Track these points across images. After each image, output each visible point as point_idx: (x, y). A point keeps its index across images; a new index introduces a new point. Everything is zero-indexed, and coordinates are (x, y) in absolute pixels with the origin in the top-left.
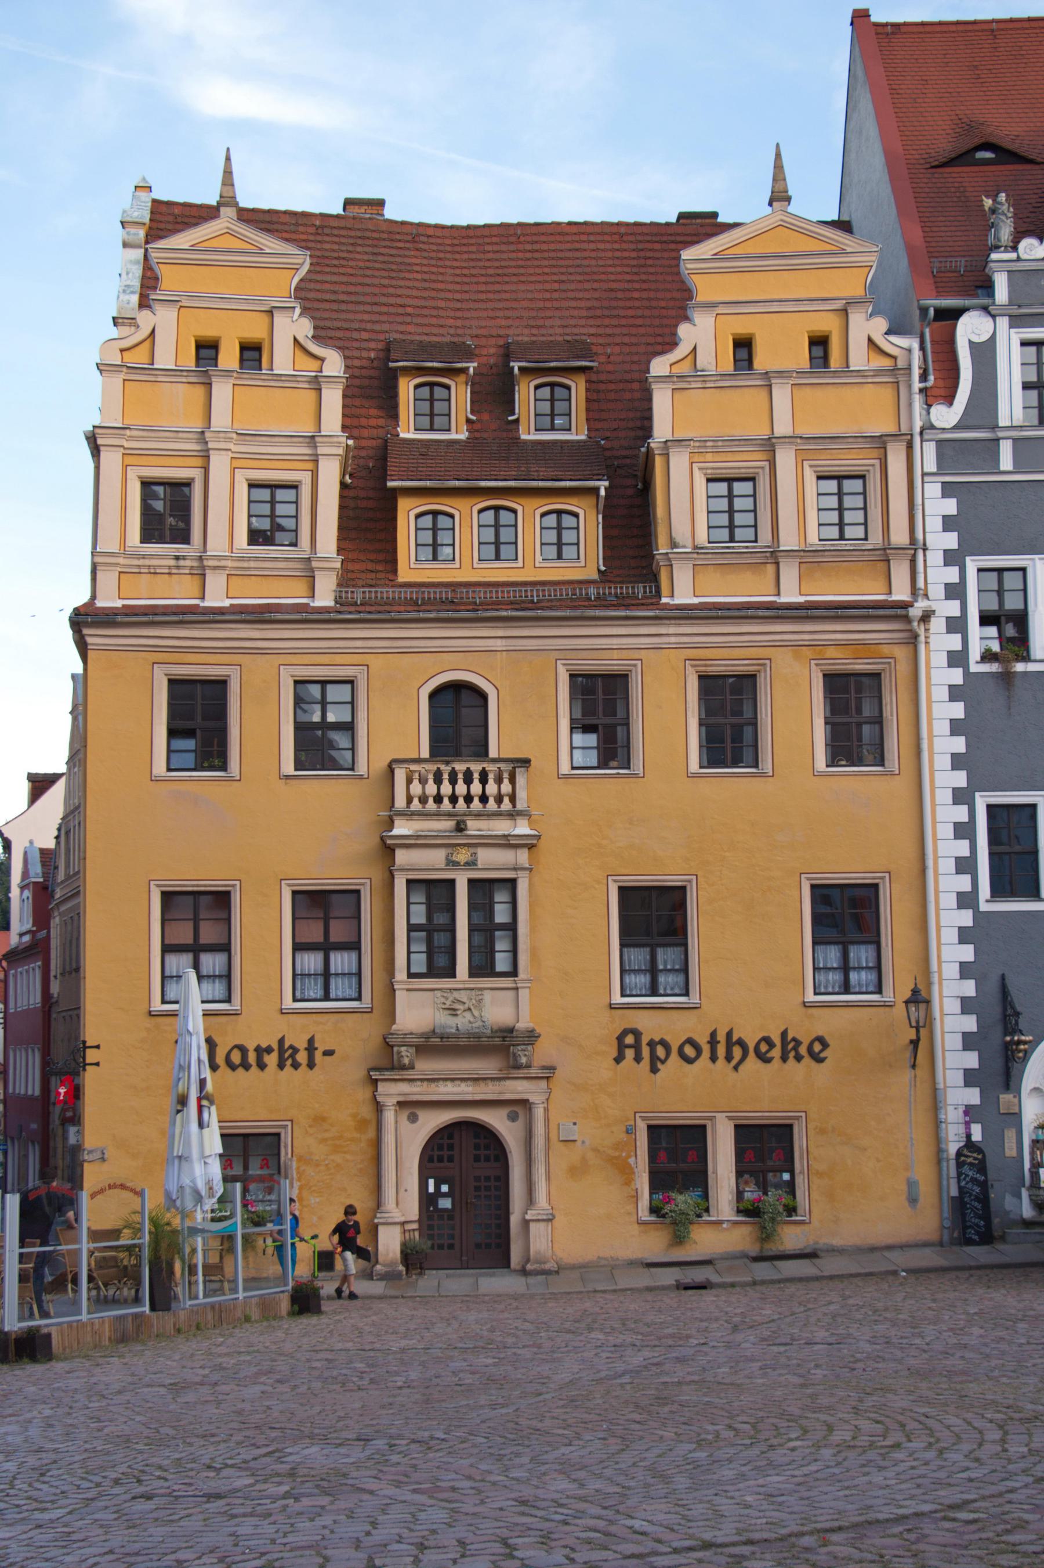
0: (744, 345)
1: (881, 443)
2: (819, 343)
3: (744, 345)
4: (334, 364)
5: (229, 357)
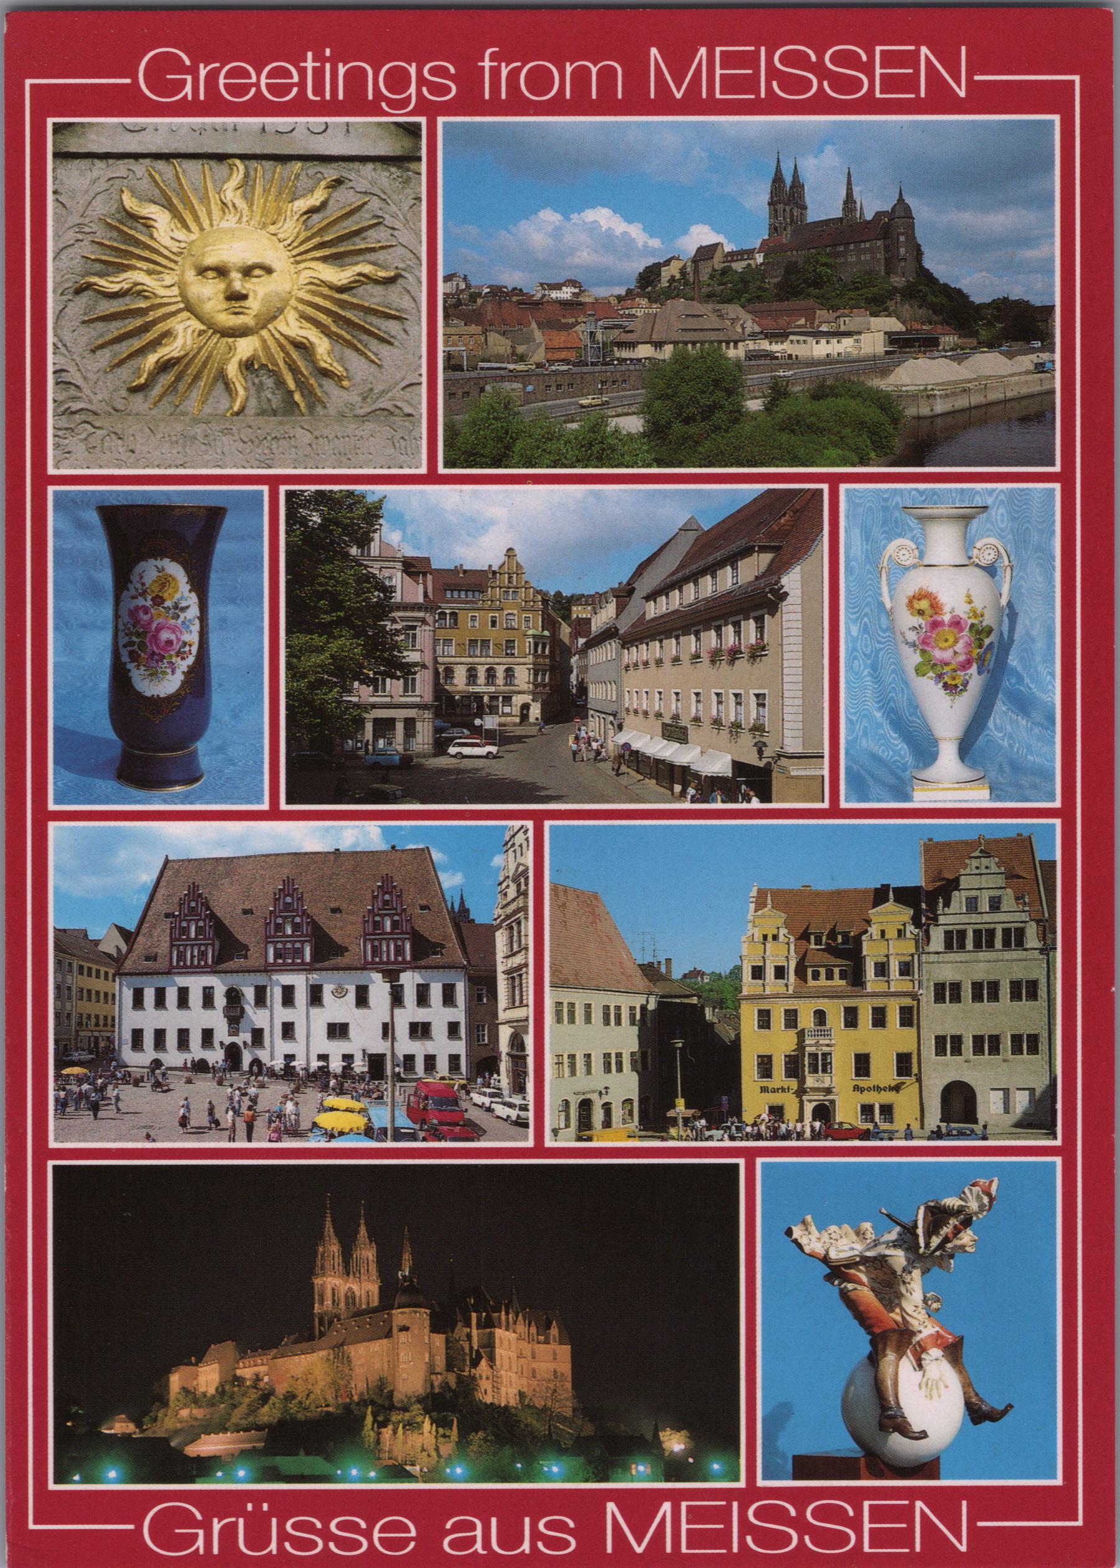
0: (883, 933)
1: (912, 955)
2: (899, 931)
3: (883, 933)
4: (792, 939)
5: (770, 938)
